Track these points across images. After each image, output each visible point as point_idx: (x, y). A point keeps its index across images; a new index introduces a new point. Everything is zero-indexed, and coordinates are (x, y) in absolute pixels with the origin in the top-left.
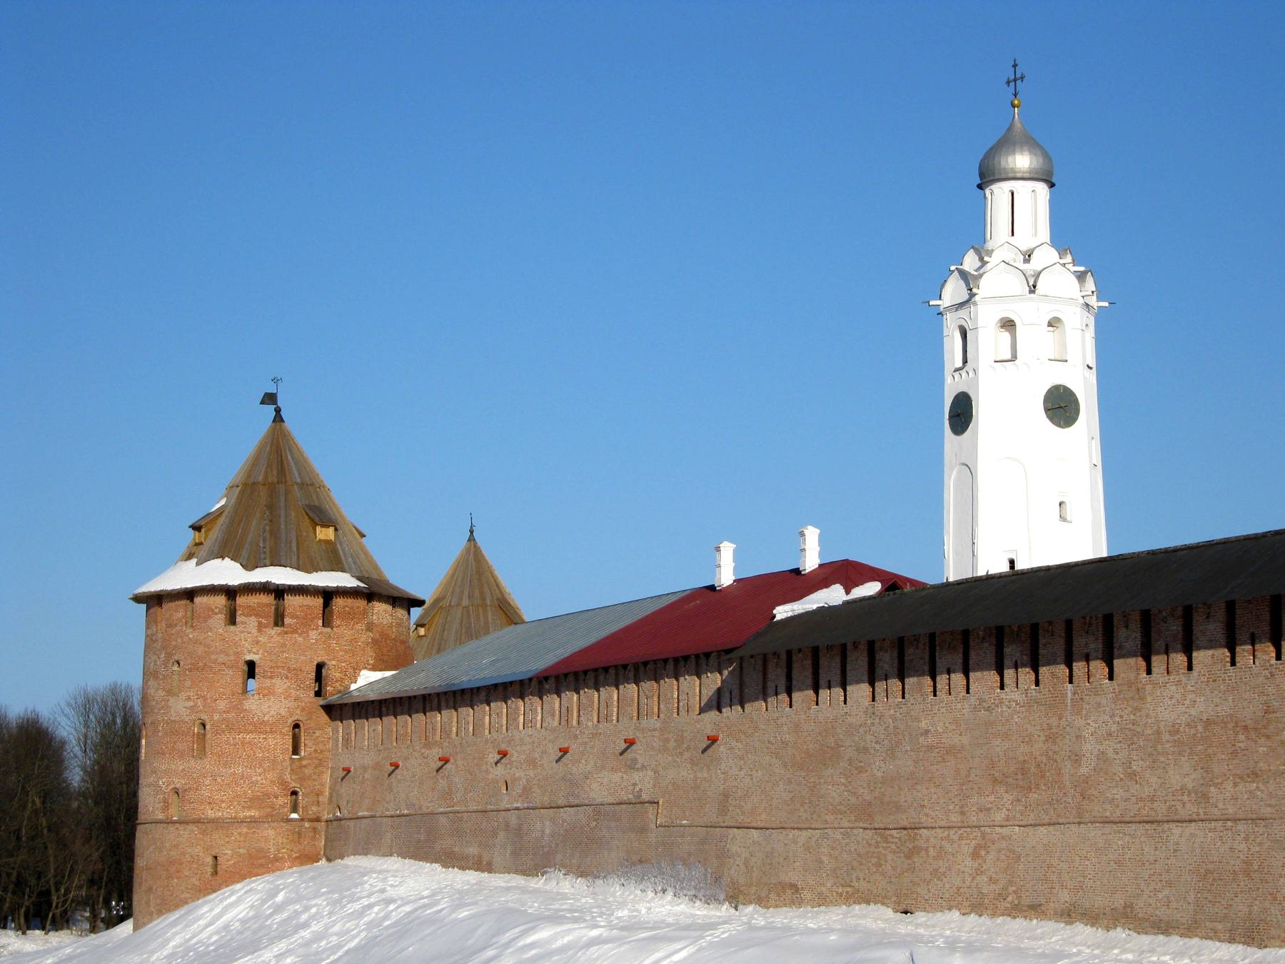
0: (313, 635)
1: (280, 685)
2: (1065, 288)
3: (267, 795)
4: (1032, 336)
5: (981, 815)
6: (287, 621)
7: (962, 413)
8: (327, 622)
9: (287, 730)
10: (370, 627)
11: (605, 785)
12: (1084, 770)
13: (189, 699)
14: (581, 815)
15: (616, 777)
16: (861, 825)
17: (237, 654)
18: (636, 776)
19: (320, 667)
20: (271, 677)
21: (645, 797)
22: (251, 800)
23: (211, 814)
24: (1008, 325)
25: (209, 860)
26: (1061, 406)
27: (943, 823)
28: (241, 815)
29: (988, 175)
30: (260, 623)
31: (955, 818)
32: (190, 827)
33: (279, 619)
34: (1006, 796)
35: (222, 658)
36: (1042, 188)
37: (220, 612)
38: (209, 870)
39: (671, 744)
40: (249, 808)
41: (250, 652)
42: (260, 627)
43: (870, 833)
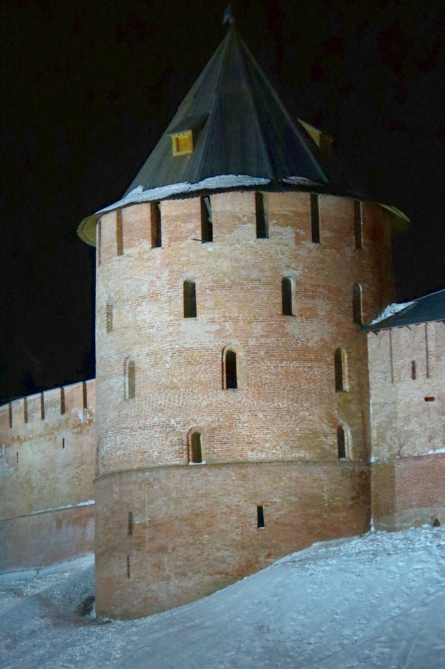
3: (316, 434)
6: (324, 234)
9: (330, 358)
13: (212, 321)
20: (313, 297)
22: (299, 438)
23: (252, 456)
25: (254, 511)
28: (290, 456)
30: (297, 234)
32: (225, 470)
37: (250, 221)
38: (255, 521)
40: (299, 448)
41: (288, 267)
42: (298, 239)
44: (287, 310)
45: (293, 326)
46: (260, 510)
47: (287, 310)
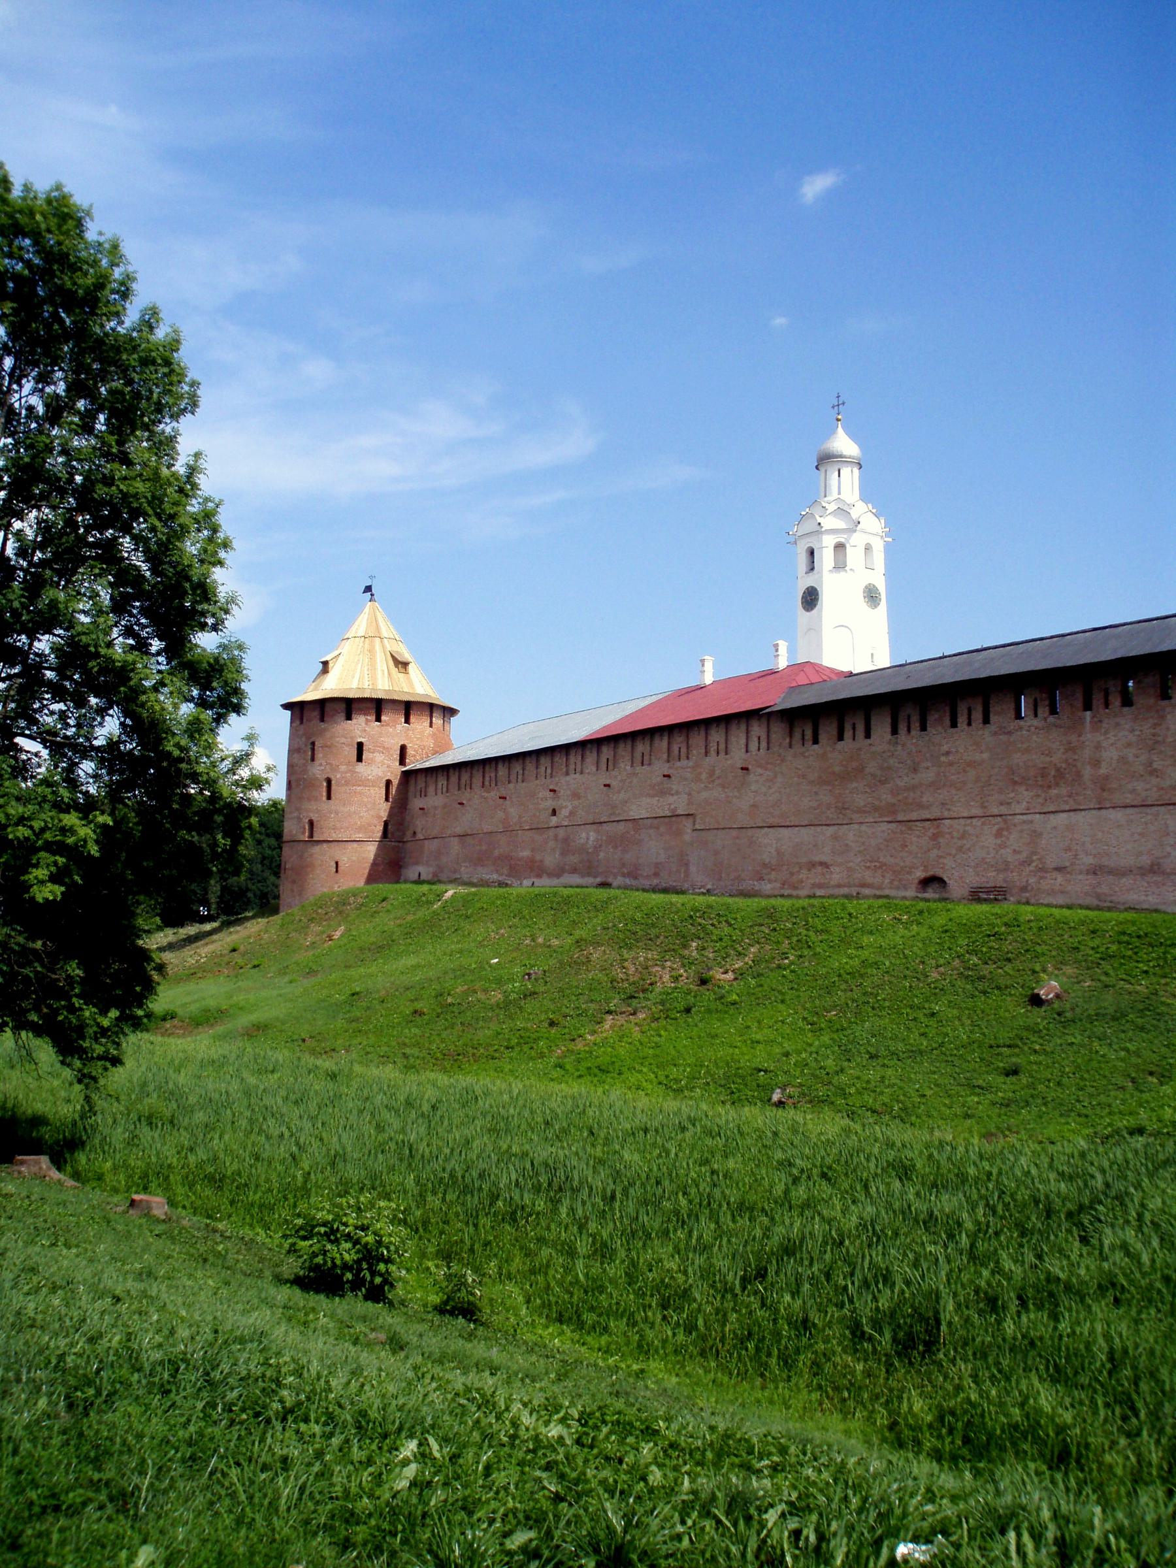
0: (399, 727)
1: (379, 757)
2: (872, 526)
4: (854, 555)
5: (1002, 808)
7: (811, 599)
8: (407, 721)
9: (383, 785)
10: (431, 726)
11: (641, 808)
12: (1103, 771)
14: (621, 827)
15: (654, 801)
16: (886, 819)
17: (352, 738)
18: (671, 799)
19: (403, 749)
21: (680, 812)
23: (334, 837)
24: (840, 547)
26: (871, 596)
27: (965, 815)
29: (826, 459)
31: (977, 811)
33: (378, 719)
34: (1026, 793)
35: (343, 740)
36: (856, 470)
39: (704, 776)
43: (894, 825)
44: (360, 759)
45: (360, 767)
46: (337, 863)
47: (360, 759)
